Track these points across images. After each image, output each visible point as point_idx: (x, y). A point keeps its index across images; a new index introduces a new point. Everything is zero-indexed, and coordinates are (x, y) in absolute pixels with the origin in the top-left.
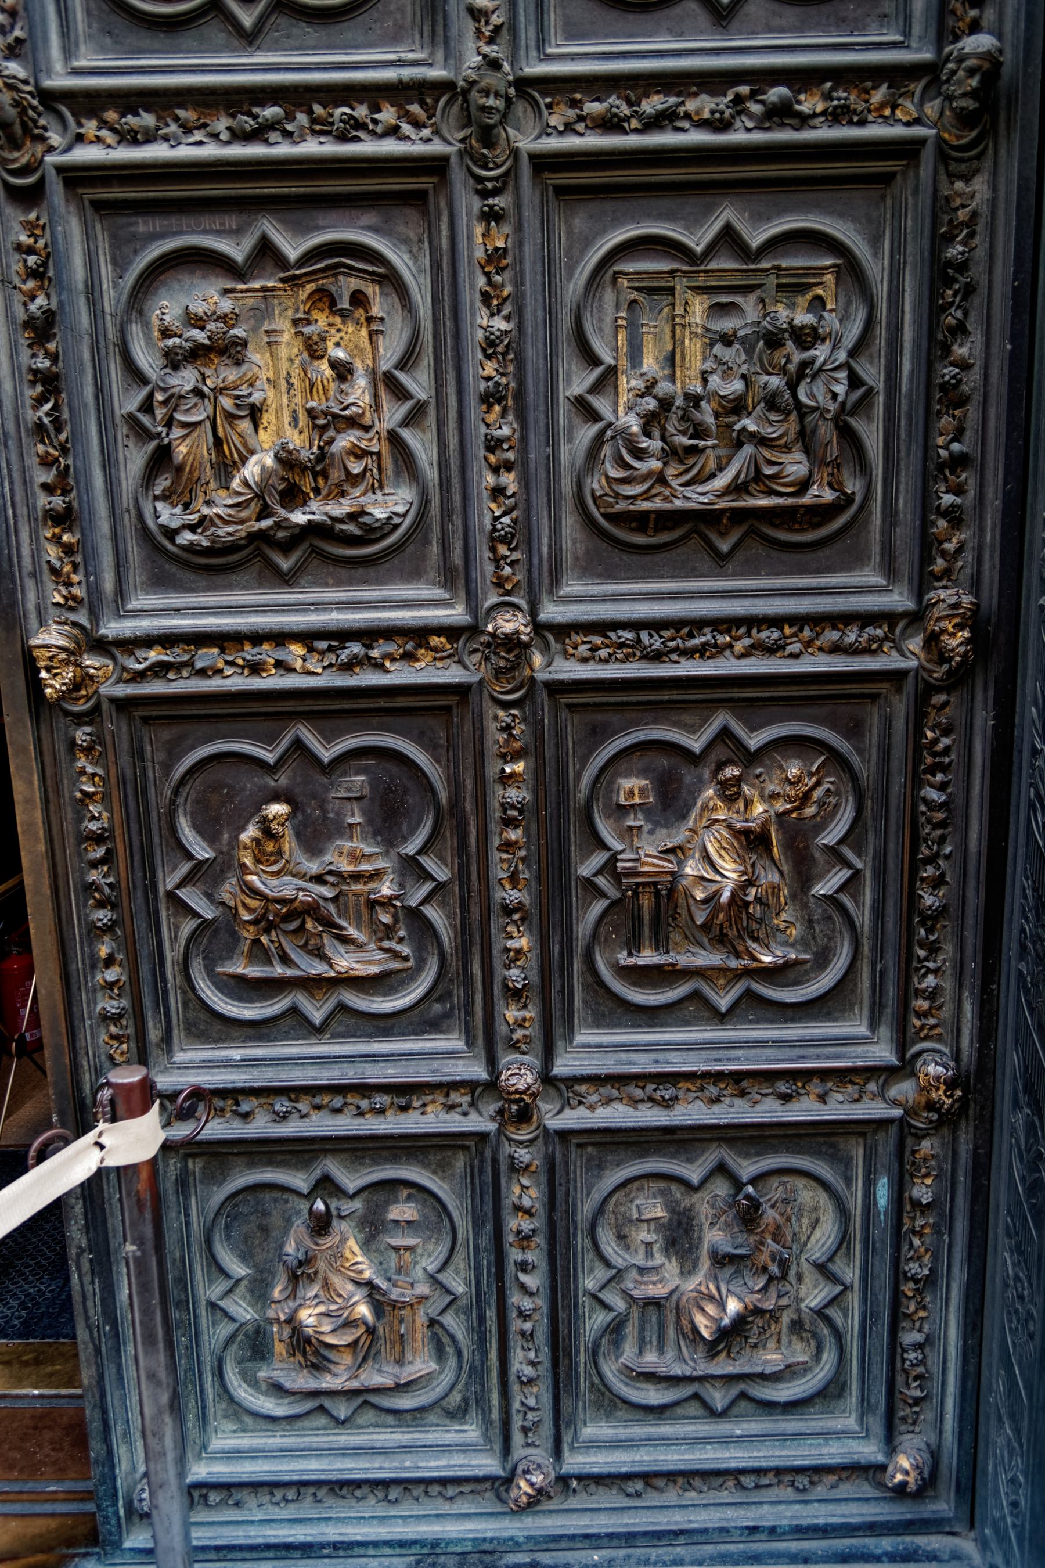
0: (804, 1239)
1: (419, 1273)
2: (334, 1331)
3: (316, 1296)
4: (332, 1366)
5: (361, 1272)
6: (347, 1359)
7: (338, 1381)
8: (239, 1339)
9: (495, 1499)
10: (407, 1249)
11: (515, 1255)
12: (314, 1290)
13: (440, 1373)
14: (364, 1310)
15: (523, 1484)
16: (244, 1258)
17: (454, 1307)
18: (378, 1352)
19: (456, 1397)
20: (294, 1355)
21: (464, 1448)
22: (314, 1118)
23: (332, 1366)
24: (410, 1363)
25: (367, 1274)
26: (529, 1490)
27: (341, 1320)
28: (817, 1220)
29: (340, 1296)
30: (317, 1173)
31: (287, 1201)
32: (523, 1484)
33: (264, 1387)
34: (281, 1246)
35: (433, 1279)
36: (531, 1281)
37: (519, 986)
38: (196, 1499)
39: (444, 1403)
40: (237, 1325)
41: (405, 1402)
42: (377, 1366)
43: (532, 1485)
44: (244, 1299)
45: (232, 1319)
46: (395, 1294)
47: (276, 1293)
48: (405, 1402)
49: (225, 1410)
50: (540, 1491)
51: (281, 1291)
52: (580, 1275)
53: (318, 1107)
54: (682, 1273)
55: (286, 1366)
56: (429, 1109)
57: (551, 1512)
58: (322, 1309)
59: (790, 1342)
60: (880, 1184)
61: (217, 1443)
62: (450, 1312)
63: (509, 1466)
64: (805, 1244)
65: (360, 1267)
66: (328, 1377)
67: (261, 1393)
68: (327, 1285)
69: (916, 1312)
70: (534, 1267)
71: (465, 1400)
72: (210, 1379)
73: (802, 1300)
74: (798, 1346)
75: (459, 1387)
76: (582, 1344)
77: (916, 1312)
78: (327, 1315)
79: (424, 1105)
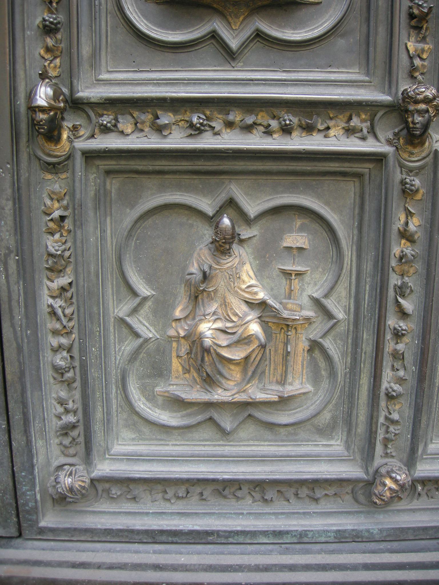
1: (305, 300)
2: (228, 346)
3: (214, 313)
4: (223, 381)
5: (256, 293)
6: (236, 373)
7: (229, 394)
8: (141, 356)
9: (352, 501)
10: (299, 274)
11: (394, 280)
12: (214, 307)
13: (315, 394)
14: (255, 328)
15: (388, 482)
16: (149, 281)
17: (333, 333)
18: (263, 372)
19: (326, 416)
20: (189, 371)
21: (332, 459)
22: (225, 136)
23: (223, 381)
24: (291, 384)
25: (261, 295)
26: (394, 486)
27: (235, 338)
29: (236, 315)
30: (223, 197)
31: (191, 226)
32: (388, 482)
33: (160, 400)
34: (185, 267)
35: (317, 303)
36: (407, 305)
37: (426, 10)
38: (100, 492)
39: (316, 421)
40: (141, 340)
41: (283, 418)
42: (261, 386)
43: (396, 481)
44: (148, 319)
45: (137, 335)
46: (285, 314)
47: (178, 313)
48: (283, 418)
49: (126, 420)
50: (402, 487)
51: (182, 310)
53: (229, 125)
55: (181, 382)
56: (332, 132)
57: (399, 511)
58: (219, 325)
61: (118, 448)
62: (330, 337)
63: (371, 471)
65: (255, 289)
66: (220, 391)
67: (157, 406)
68: (225, 304)
70: (412, 291)
71: (334, 419)
72: (114, 391)
75: (330, 406)
78: (224, 331)
79: (328, 128)
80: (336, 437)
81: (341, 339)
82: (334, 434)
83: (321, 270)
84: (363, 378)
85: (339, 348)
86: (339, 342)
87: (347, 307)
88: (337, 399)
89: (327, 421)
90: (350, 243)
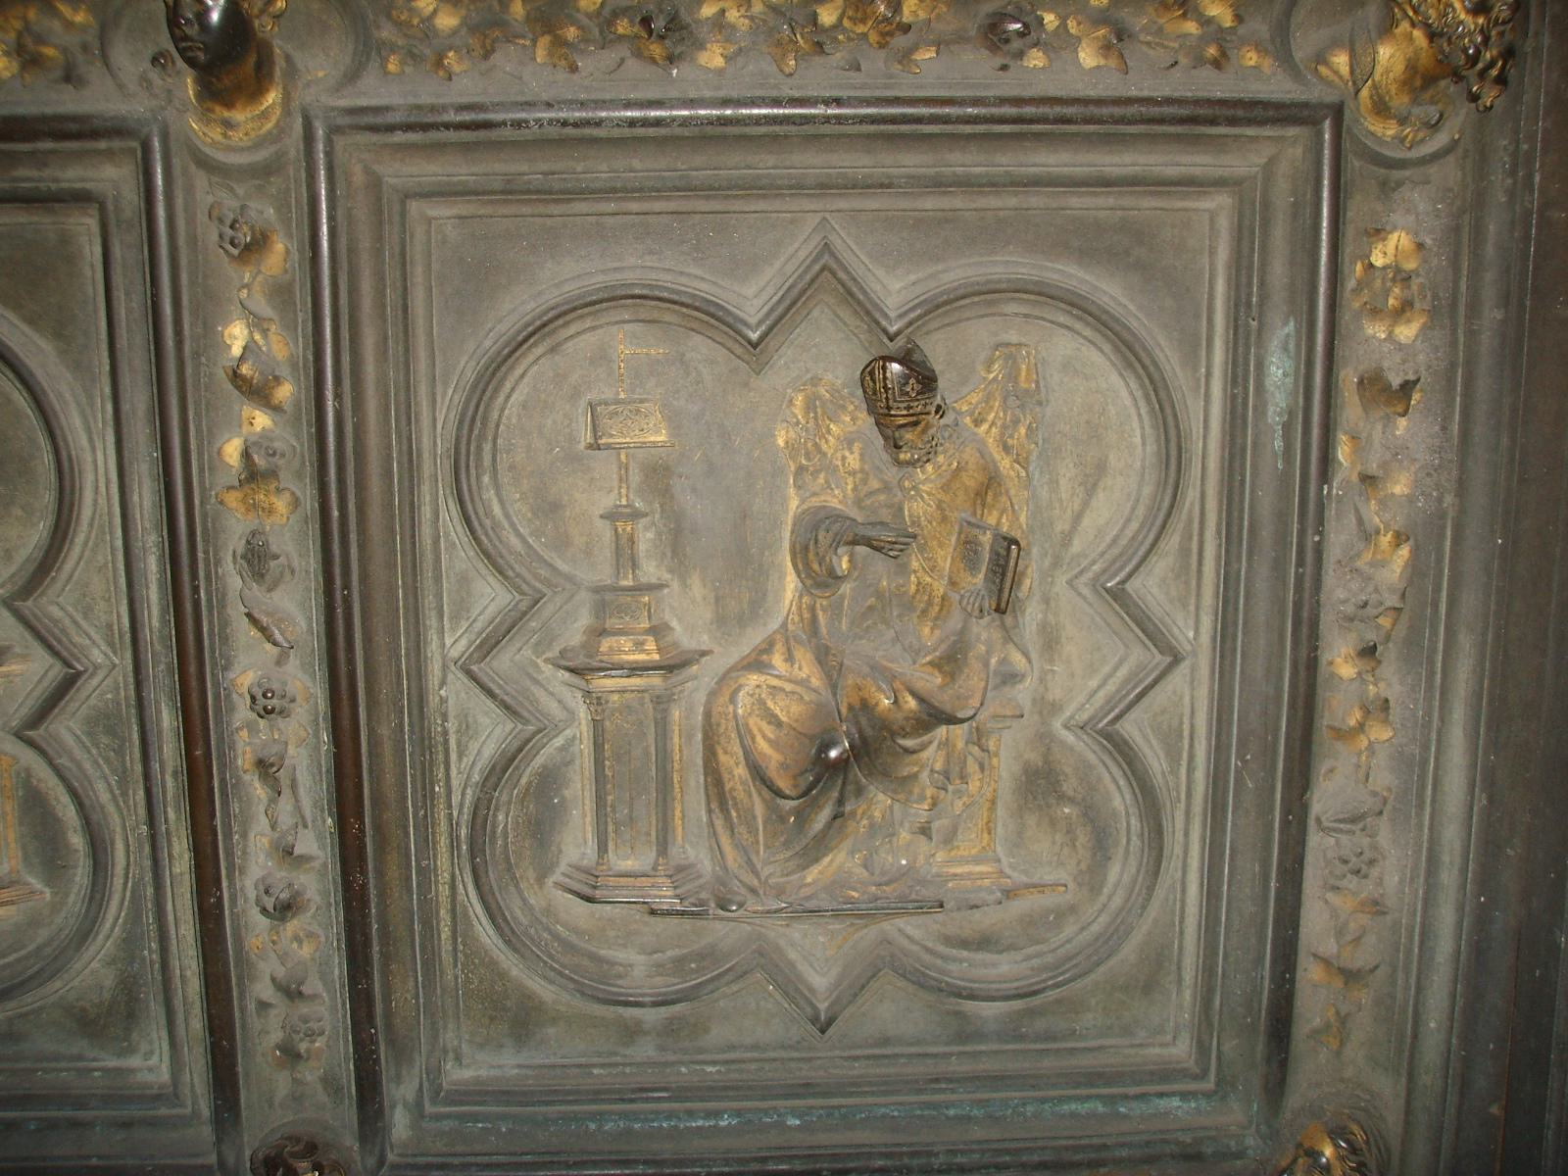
0: (1062, 526)
28: (1101, 467)
52: (432, 622)
54: (720, 620)
59: (1020, 834)
60: (1274, 345)
64: (1067, 539)
69: (1361, 727)
73: (1055, 708)
74: (1043, 843)
76: (443, 826)
77: (1361, 727)
80: (144, 1047)
81: (111, 731)
82: (135, 1035)
83: (19, 512)
84: (181, 856)
85: (107, 760)
86: (105, 740)
87: (116, 627)
88: (125, 922)
89: (107, 995)
90: (96, 422)
